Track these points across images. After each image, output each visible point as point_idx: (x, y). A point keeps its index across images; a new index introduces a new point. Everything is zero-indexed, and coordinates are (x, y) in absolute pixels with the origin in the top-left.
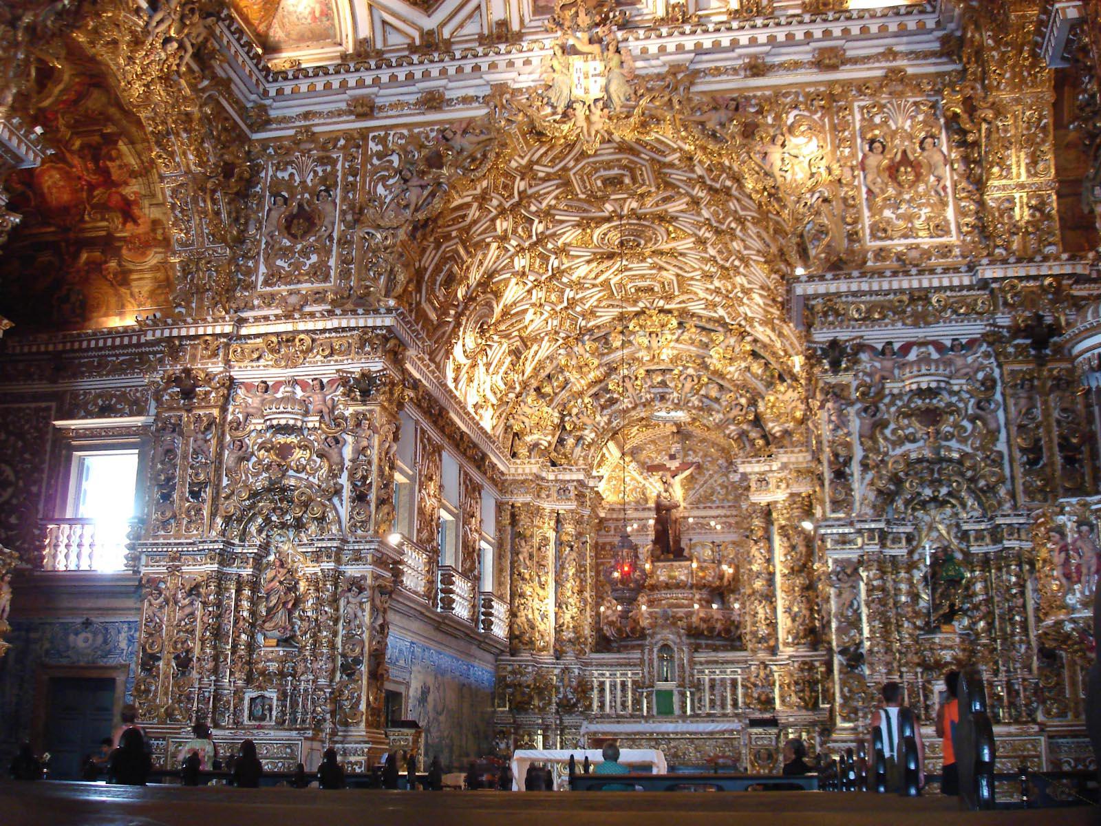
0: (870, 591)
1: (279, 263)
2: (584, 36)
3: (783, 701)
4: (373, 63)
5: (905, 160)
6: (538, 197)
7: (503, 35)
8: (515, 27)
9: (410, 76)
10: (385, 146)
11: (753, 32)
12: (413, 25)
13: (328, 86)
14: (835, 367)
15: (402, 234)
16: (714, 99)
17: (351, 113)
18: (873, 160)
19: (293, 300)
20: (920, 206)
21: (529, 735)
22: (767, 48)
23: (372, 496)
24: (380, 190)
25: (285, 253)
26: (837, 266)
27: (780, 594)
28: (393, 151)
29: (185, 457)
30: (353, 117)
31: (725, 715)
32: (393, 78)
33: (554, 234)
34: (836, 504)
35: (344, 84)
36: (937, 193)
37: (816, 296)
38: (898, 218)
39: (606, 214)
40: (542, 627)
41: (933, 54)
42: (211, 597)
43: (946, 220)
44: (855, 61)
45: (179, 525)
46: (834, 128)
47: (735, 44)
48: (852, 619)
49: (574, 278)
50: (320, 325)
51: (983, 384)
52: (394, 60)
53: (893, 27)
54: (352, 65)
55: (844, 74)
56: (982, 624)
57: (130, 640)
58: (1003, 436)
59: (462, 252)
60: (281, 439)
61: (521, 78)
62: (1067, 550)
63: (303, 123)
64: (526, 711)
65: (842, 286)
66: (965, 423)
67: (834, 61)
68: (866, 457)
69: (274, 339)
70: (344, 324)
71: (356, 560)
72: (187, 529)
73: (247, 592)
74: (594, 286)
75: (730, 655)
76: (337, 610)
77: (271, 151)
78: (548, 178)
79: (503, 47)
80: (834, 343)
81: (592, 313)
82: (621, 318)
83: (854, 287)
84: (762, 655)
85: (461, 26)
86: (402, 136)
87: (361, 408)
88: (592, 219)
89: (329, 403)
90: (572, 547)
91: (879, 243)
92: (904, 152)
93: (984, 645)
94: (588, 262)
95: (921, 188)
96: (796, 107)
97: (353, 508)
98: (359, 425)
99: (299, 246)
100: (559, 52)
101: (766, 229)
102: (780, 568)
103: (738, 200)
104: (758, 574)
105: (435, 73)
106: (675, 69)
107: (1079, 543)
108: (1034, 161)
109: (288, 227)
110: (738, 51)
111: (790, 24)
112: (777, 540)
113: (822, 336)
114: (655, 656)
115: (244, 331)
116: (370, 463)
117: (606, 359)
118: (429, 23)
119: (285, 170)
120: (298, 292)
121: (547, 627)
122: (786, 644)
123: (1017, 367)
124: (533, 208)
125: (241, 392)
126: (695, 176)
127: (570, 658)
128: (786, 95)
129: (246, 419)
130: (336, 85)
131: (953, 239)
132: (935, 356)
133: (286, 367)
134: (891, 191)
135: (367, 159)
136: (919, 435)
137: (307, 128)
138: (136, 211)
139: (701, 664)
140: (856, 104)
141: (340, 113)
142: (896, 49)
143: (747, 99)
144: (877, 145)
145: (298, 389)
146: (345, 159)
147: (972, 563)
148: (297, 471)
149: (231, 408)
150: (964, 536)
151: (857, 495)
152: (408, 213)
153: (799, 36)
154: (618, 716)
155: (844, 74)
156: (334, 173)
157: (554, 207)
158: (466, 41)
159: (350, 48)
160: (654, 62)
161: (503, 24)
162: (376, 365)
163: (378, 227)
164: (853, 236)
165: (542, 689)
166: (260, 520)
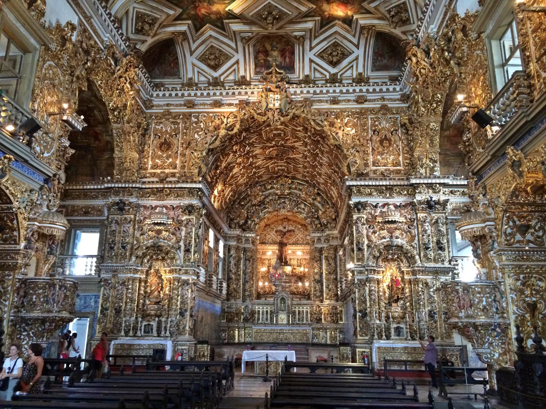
0: (370, 291)
1: (157, 161)
2: (274, 85)
3: (325, 320)
4: (194, 88)
5: (386, 138)
6: (249, 139)
7: (243, 82)
8: (248, 79)
9: (208, 94)
10: (198, 120)
11: (335, 88)
14: (359, 210)
15: (204, 154)
16: (319, 112)
17: (185, 106)
18: (374, 138)
19: (162, 175)
20: (390, 156)
21: (233, 331)
22: (339, 94)
23: (192, 250)
24: (196, 136)
25: (159, 157)
26: (361, 175)
27: (324, 280)
28: (201, 122)
29: (120, 233)
30: (186, 107)
31: (303, 324)
32: (202, 94)
33: (253, 151)
34: (358, 260)
35: (183, 95)
36: (397, 151)
37: (353, 186)
38: (382, 159)
39: (272, 145)
41: (398, 100)
42: (130, 286)
43: (400, 162)
44: (370, 101)
45: (117, 258)
46: (361, 125)
47: (328, 92)
50: (173, 186)
55: (366, 105)
56: (408, 304)
57: (96, 302)
58: (417, 238)
59: (221, 157)
60: (158, 227)
61: (250, 98)
63: (166, 108)
64: (232, 321)
65: (363, 183)
66: (403, 233)
67: (363, 101)
69: (155, 190)
71: (186, 273)
72: (120, 260)
73: (143, 284)
74: (263, 168)
75: (306, 302)
76: (178, 292)
77: (153, 117)
78: (254, 132)
79: (244, 87)
80: (359, 203)
81: (261, 176)
83: (367, 183)
85: (228, 76)
86: (205, 116)
87: (188, 217)
88: (267, 146)
89: (177, 215)
91: (375, 168)
92: (386, 135)
94: (263, 160)
95: (391, 149)
96: (348, 116)
97: (185, 254)
98: (187, 223)
99: (165, 155)
100: (265, 91)
101: (331, 155)
103: (322, 145)
104: (317, 274)
105: (218, 94)
106: (306, 100)
107: (464, 296)
108: (432, 141)
109: (161, 147)
110: (329, 94)
111: (348, 86)
112: (324, 261)
113: (354, 200)
114: (279, 302)
115: (144, 186)
116: (192, 238)
117: (264, 193)
118: (216, 75)
119: (159, 125)
120: (165, 173)
122: (326, 299)
124: (247, 142)
125: (142, 209)
126: (307, 135)
127: (248, 302)
128: (344, 112)
129: (144, 219)
130: (180, 95)
131: (401, 168)
132: (394, 209)
133: (160, 200)
134: (380, 149)
135: (191, 124)
136: (387, 237)
138: (100, 137)
139: (295, 305)
140: (369, 117)
141: (181, 105)
142: (385, 97)
143: (331, 112)
144: (376, 132)
145: (164, 209)
146: (182, 123)
148: (164, 239)
149: (138, 215)
150: (402, 272)
151: (366, 257)
152: (207, 145)
153: (351, 91)
154: (265, 324)
155: (366, 105)
156: (178, 128)
157: (255, 142)
158: (230, 83)
160: (298, 96)
161: (244, 77)
163: (196, 150)
164: (366, 165)
165: (238, 314)
166: (148, 257)
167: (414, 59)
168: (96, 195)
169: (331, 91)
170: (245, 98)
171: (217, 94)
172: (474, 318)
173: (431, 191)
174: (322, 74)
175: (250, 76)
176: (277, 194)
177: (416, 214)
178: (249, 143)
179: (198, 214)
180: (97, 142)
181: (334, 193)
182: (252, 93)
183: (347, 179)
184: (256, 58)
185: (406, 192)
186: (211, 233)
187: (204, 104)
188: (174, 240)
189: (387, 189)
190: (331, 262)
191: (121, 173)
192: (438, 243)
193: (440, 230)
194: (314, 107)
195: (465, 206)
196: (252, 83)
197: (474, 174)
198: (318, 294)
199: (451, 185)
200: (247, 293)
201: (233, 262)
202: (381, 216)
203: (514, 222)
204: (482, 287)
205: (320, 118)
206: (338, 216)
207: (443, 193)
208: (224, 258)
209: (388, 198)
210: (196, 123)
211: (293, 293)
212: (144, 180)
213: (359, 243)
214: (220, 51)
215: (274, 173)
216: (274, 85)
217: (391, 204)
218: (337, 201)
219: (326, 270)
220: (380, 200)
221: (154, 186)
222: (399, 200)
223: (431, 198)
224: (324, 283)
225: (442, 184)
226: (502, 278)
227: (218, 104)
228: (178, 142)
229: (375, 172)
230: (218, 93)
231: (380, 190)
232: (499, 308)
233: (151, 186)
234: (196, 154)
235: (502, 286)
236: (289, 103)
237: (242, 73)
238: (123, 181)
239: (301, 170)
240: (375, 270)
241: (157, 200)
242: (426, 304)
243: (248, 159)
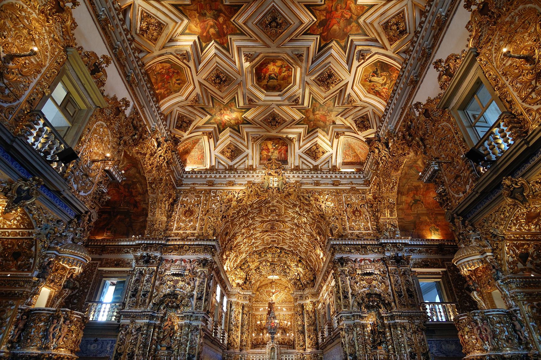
1: (181, 224)
2: (274, 171)
7: (251, 169)
8: (254, 167)
9: (225, 176)
10: (216, 194)
12: (227, 164)
13: (201, 176)
14: (342, 264)
18: (348, 209)
19: (184, 235)
24: (213, 206)
25: (183, 221)
26: (341, 237)
27: (306, 331)
32: (220, 176)
34: (345, 307)
35: (206, 177)
37: (336, 244)
38: (356, 225)
40: (236, 341)
43: (369, 227)
44: (342, 184)
46: (338, 200)
48: (352, 344)
50: (192, 243)
51: (383, 272)
56: (390, 346)
58: (390, 288)
60: (176, 278)
62: (480, 329)
65: (344, 243)
68: (352, 292)
79: (251, 172)
80: (342, 258)
82: (264, 249)
83: (347, 243)
84: (301, 351)
85: (239, 165)
86: (221, 192)
88: (265, 221)
93: (392, 354)
97: (197, 302)
102: (306, 324)
104: (300, 325)
105: (232, 176)
106: (297, 182)
109: (185, 214)
113: (338, 256)
115: (168, 243)
116: (204, 287)
118: (231, 163)
121: (238, 340)
122: (308, 348)
123: (392, 268)
125: (164, 262)
127: (244, 352)
129: (165, 271)
130: (204, 176)
131: (371, 232)
137: (194, 187)
141: (203, 184)
147: (384, 326)
153: (329, 177)
159: (208, 167)
161: (252, 166)
162: (209, 257)
163: (213, 216)
164: (344, 229)
167: (377, 151)
169: (315, 177)
170: (252, 179)
172: (501, 351)
174: (307, 165)
176: (269, 262)
177: (387, 267)
179: (211, 268)
180: (135, 209)
181: (313, 258)
182: (258, 176)
186: (219, 289)
187: (221, 184)
188: (189, 288)
189: (362, 247)
190: (311, 314)
191: (151, 233)
192: (408, 290)
193: (408, 281)
194: (303, 187)
195: (423, 261)
197: (458, 215)
198: (302, 343)
199: (410, 245)
200: (244, 343)
202: (360, 269)
203: (514, 251)
204: (499, 316)
205: (307, 195)
206: (315, 278)
208: (227, 312)
209: (363, 255)
210: (214, 197)
211: (281, 344)
213: (344, 291)
214: (236, 147)
215: (267, 244)
216: (274, 171)
217: (366, 260)
218: (315, 264)
219: (308, 322)
223: (398, 254)
224: (306, 334)
226: (516, 306)
227: (232, 184)
228: (199, 212)
229: (352, 234)
232: (521, 337)
234: (212, 219)
235: (519, 315)
236: (285, 184)
237: (250, 164)
239: (287, 241)
240: (360, 316)
241: (178, 255)
242: (406, 346)
243: (250, 230)
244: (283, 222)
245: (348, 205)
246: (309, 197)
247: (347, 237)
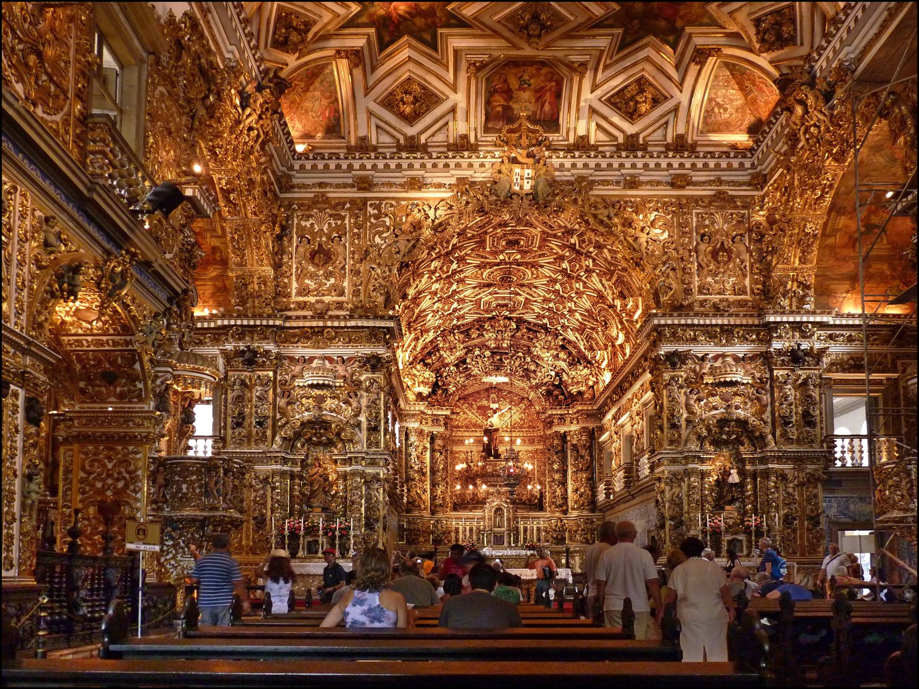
6: (460, 248)
7: (463, 146)
8: (472, 140)
26: (678, 308)
33: (461, 271)
49: (461, 296)
50: (343, 324)
52: (388, 154)
53: (724, 165)
54: (357, 154)
65: (683, 322)
69: (309, 330)
70: (360, 323)
88: (488, 263)
90: (441, 453)
94: (474, 288)
115: (287, 324)
124: (456, 255)
158: (438, 146)
161: (465, 137)
168: (199, 339)
171: (415, 166)
173: (797, 334)
175: (476, 136)
178: (460, 257)
183: (656, 315)
184: (488, 103)
185: (754, 337)
189: (722, 331)
195: (852, 358)
196: (480, 148)
199: (831, 326)
201: (414, 454)
207: (818, 339)
212: (289, 313)
220: (712, 349)
221: (308, 324)
222: (741, 349)
223: (799, 345)
225: (818, 323)
230: (417, 165)
231: (711, 333)
233: (301, 324)
238: (250, 315)
243: (451, 284)
244: (534, 265)
245: (703, 235)
246: (610, 218)
247: (693, 309)
